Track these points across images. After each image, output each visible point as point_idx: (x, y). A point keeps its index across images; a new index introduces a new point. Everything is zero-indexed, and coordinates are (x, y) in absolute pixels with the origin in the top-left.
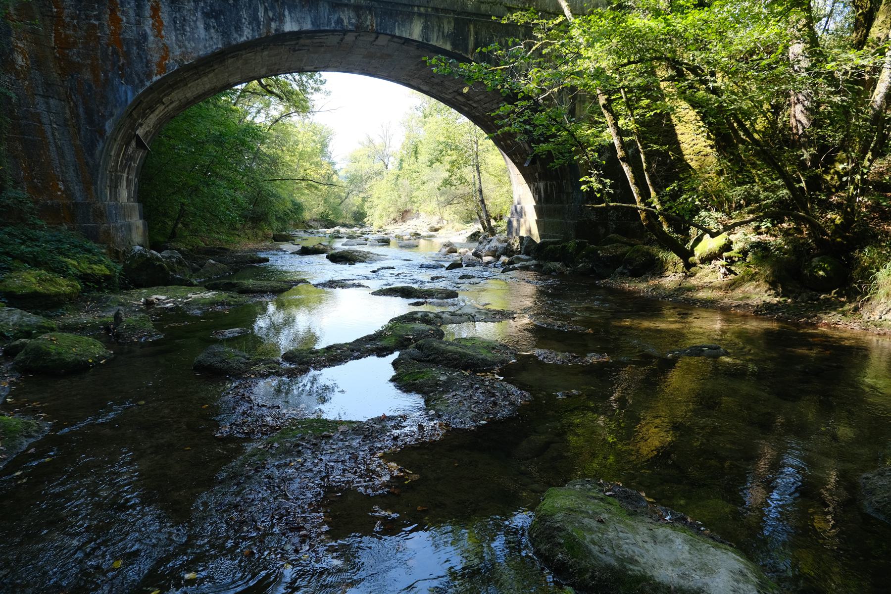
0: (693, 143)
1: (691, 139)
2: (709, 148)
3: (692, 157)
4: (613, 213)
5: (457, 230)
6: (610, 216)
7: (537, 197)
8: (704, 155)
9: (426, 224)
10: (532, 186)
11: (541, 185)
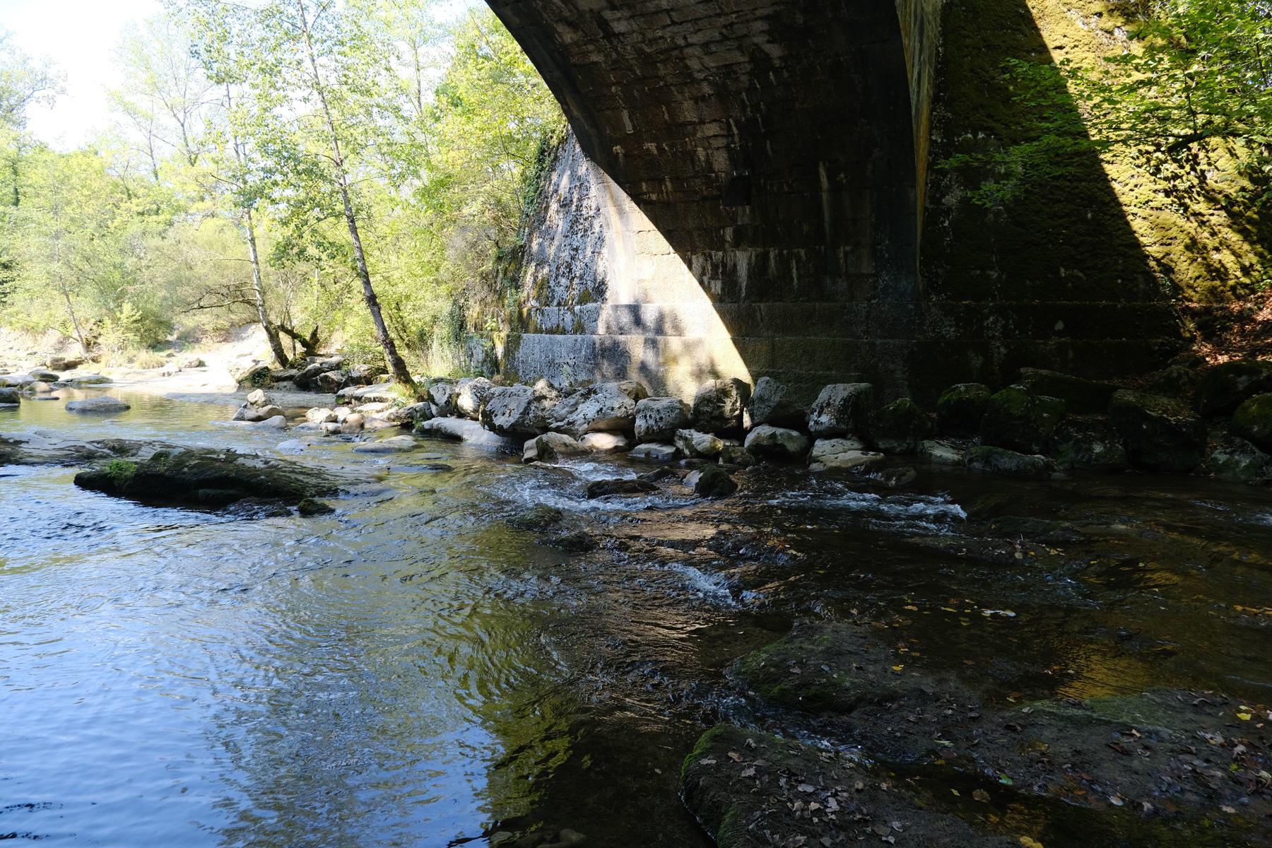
0: (1134, 181)
1: (1129, 174)
2: (1162, 195)
3: (1135, 210)
4: (995, 322)
5: (146, 366)
6: (988, 328)
7: (717, 286)
8: (1157, 209)
9: (23, 354)
10: (697, 261)
11: (742, 260)
